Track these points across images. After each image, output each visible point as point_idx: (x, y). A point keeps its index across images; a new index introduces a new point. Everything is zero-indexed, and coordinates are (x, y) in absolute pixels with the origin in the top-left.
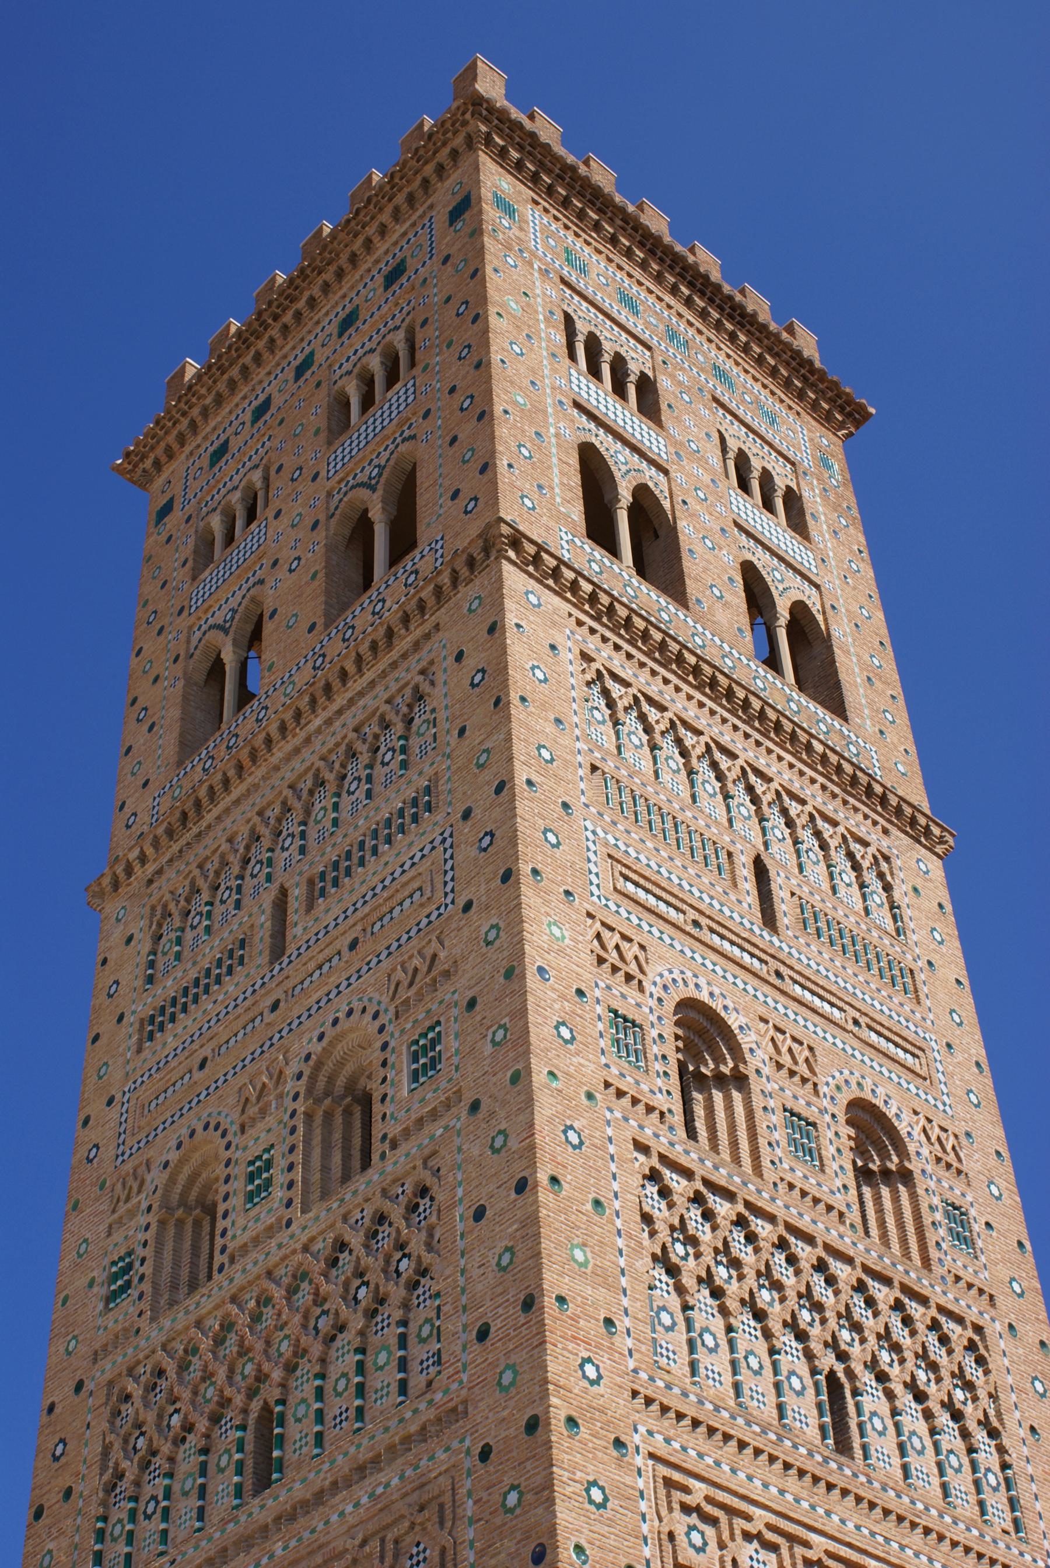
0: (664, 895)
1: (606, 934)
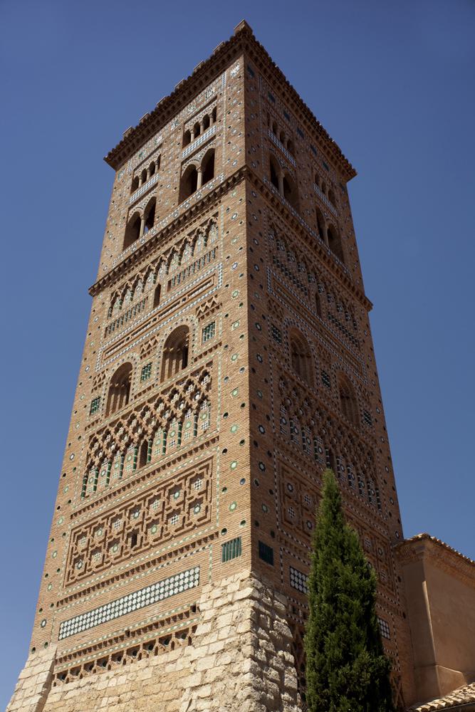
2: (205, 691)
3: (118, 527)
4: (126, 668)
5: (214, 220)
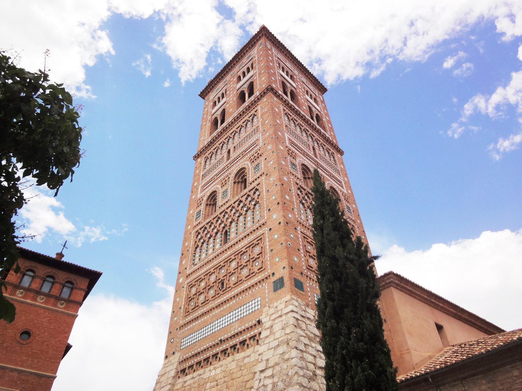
2: (269, 372)
3: (213, 278)
4: (220, 363)
5: (256, 114)
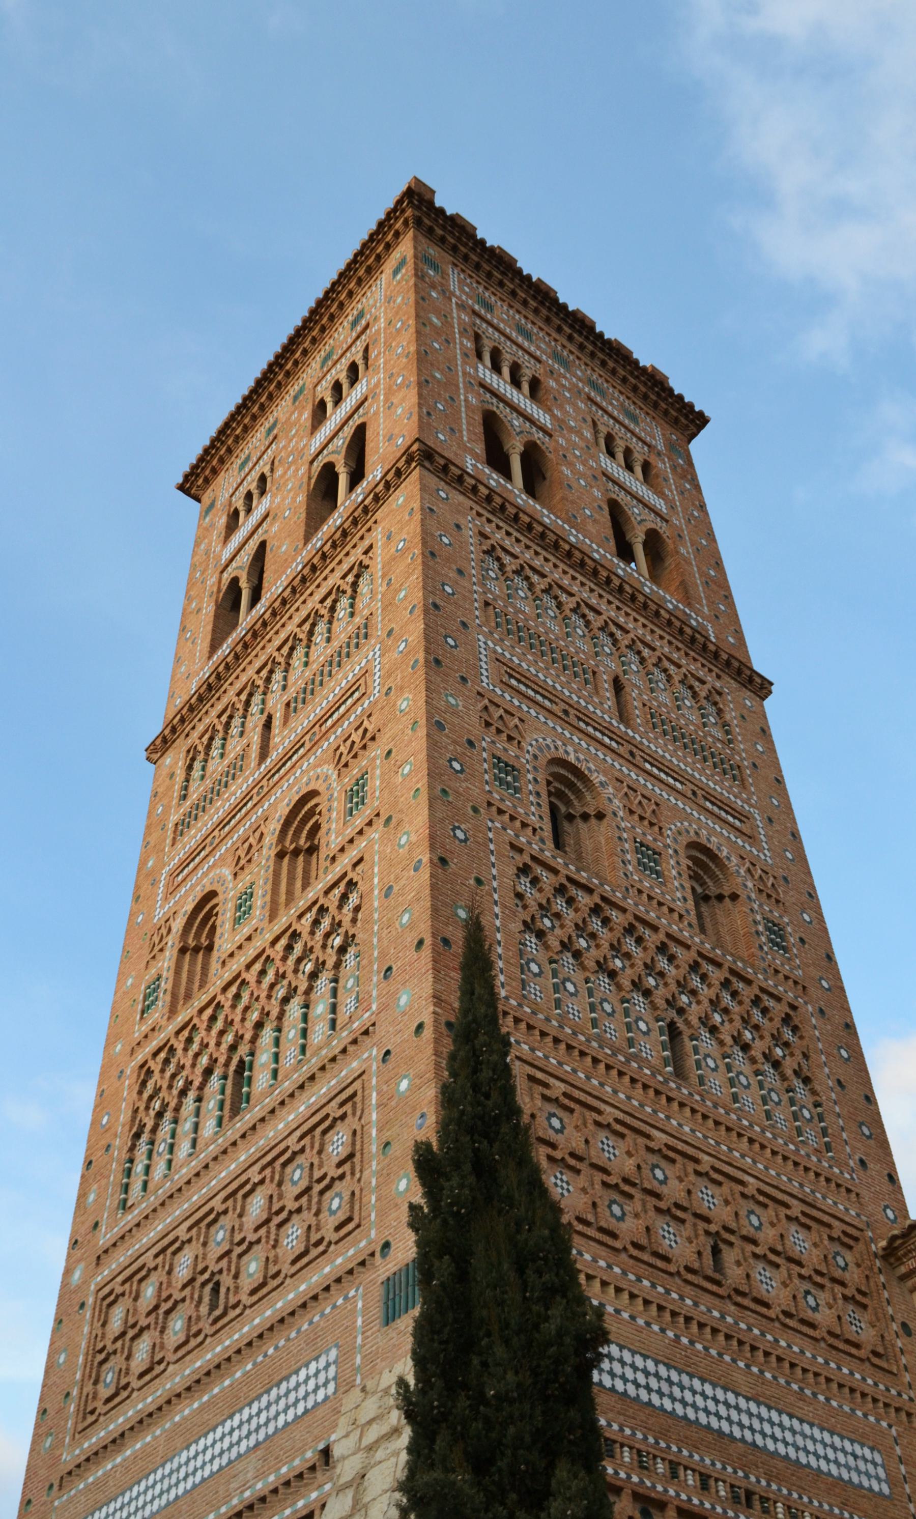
0: (540, 690)
1: (492, 708)
5: (366, 562)
